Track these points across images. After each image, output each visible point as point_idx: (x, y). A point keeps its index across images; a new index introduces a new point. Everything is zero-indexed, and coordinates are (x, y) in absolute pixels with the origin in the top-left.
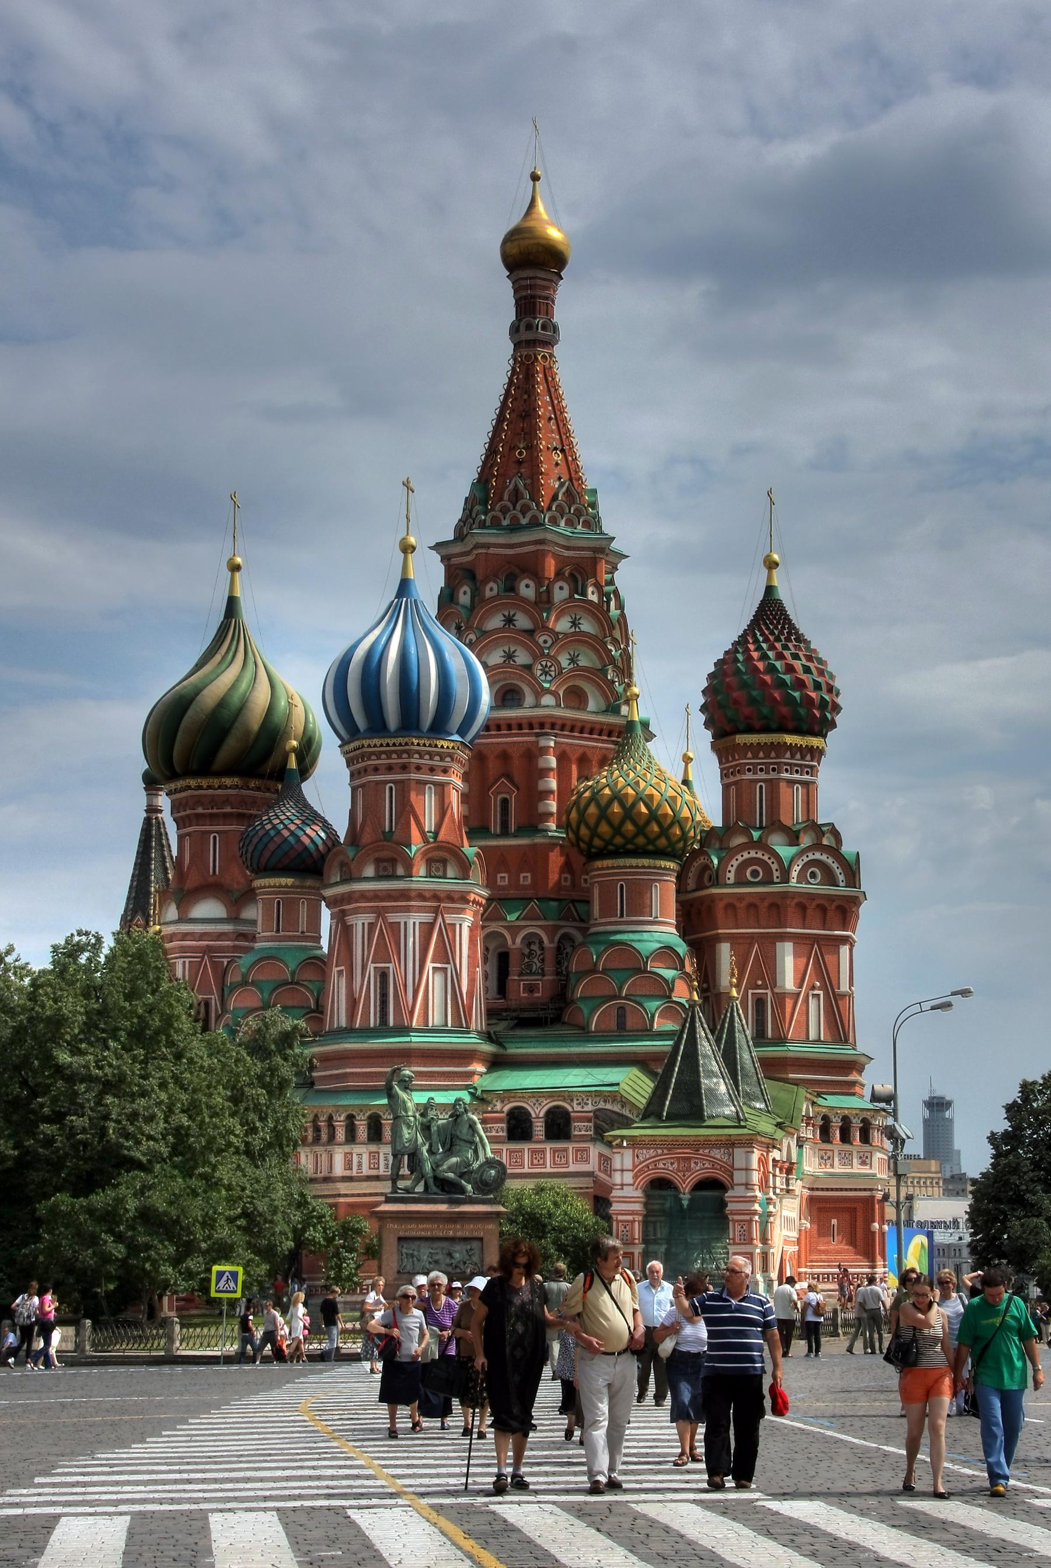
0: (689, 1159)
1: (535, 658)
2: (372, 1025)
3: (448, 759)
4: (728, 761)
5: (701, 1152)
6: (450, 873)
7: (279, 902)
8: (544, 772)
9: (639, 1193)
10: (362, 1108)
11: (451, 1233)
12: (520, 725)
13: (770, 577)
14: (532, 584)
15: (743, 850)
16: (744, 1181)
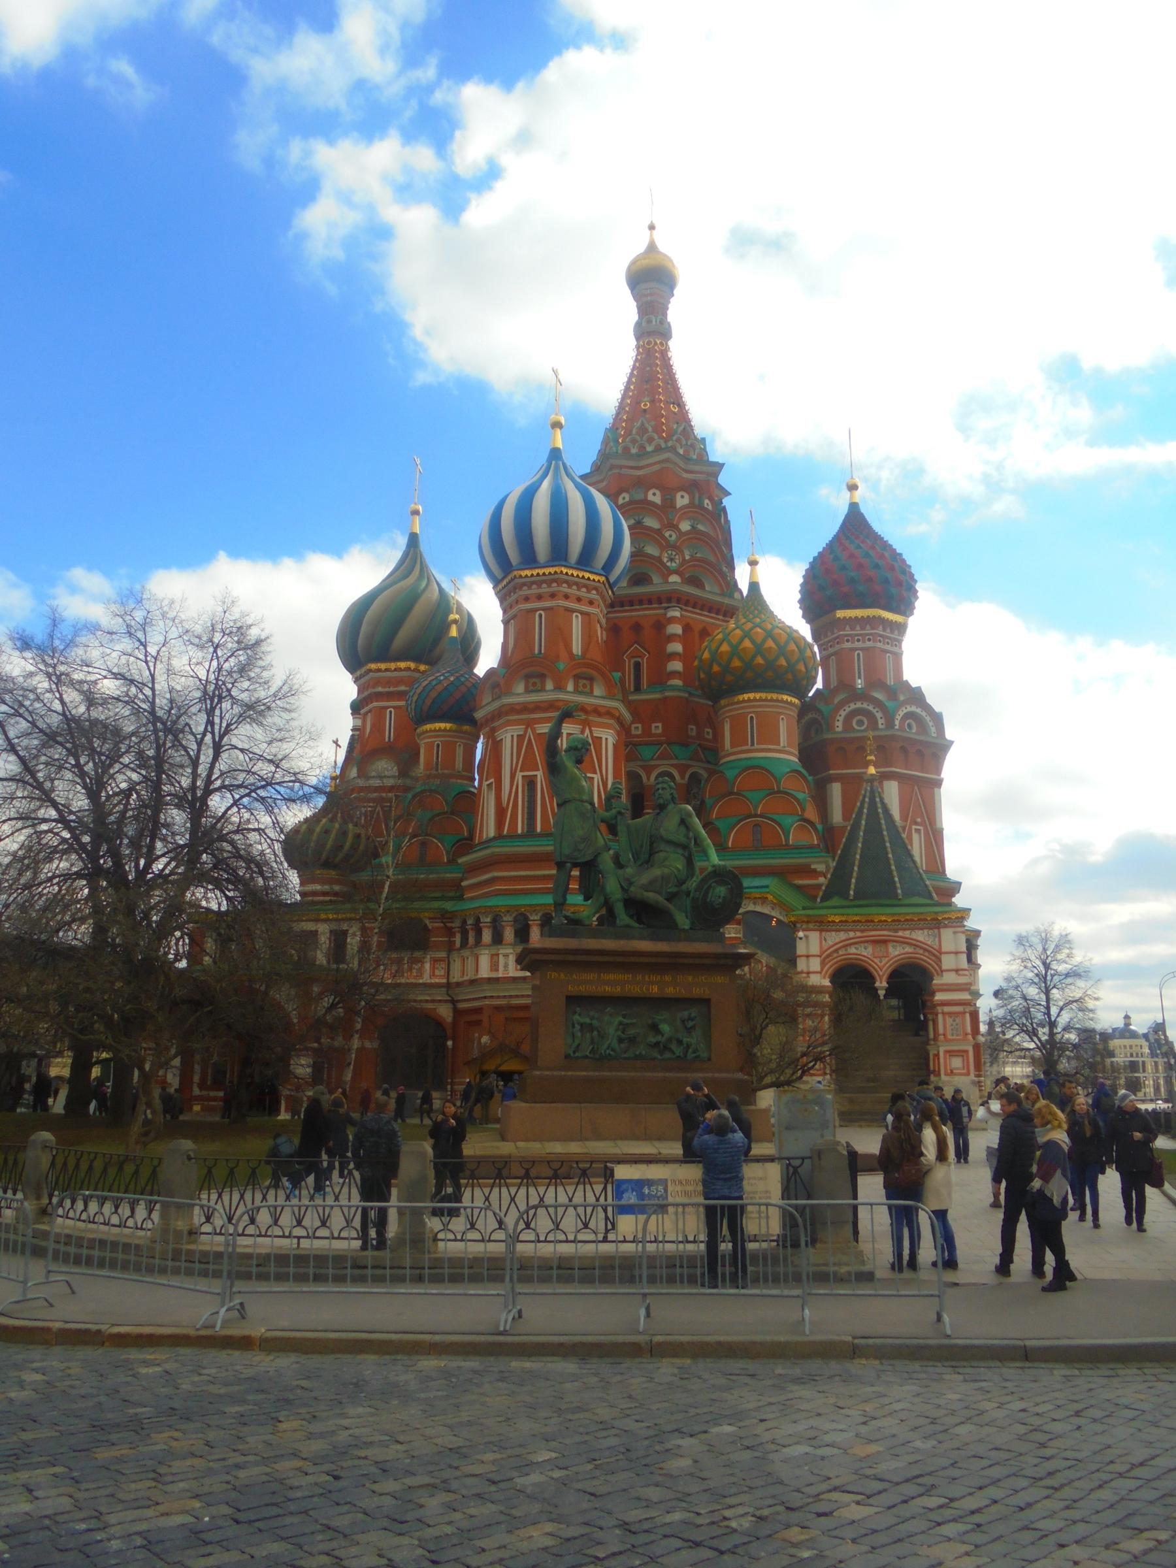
0: (885, 942)
1: (663, 548)
2: (520, 831)
3: (594, 592)
4: (826, 636)
5: (900, 933)
6: (598, 691)
7: (438, 745)
8: (672, 638)
9: (827, 982)
10: (509, 909)
11: (655, 990)
12: (648, 600)
13: (851, 497)
14: (658, 492)
15: (850, 701)
16: (954, 967)
